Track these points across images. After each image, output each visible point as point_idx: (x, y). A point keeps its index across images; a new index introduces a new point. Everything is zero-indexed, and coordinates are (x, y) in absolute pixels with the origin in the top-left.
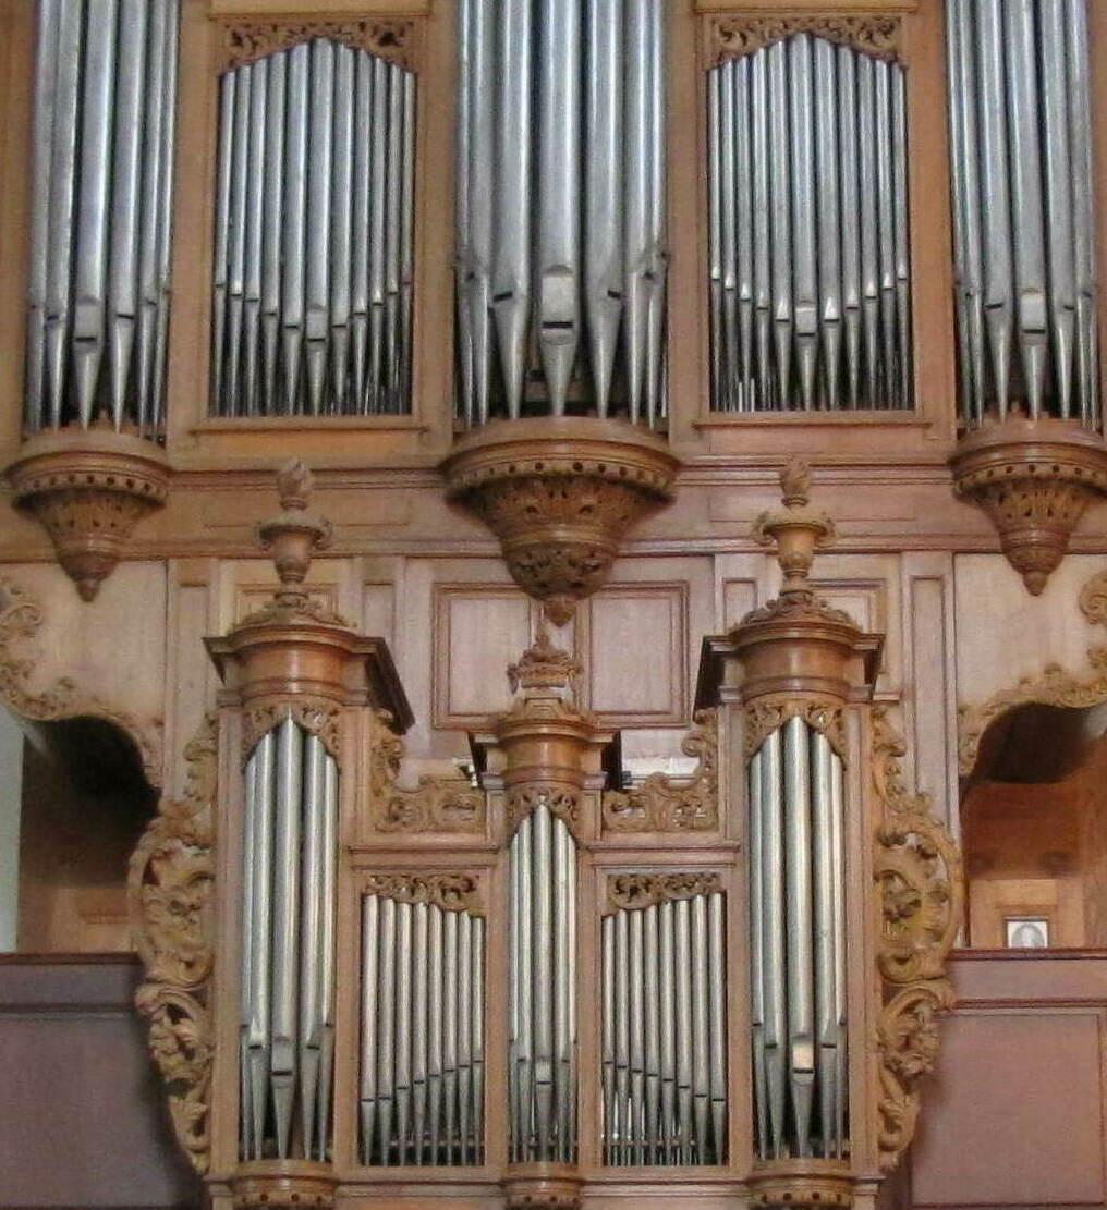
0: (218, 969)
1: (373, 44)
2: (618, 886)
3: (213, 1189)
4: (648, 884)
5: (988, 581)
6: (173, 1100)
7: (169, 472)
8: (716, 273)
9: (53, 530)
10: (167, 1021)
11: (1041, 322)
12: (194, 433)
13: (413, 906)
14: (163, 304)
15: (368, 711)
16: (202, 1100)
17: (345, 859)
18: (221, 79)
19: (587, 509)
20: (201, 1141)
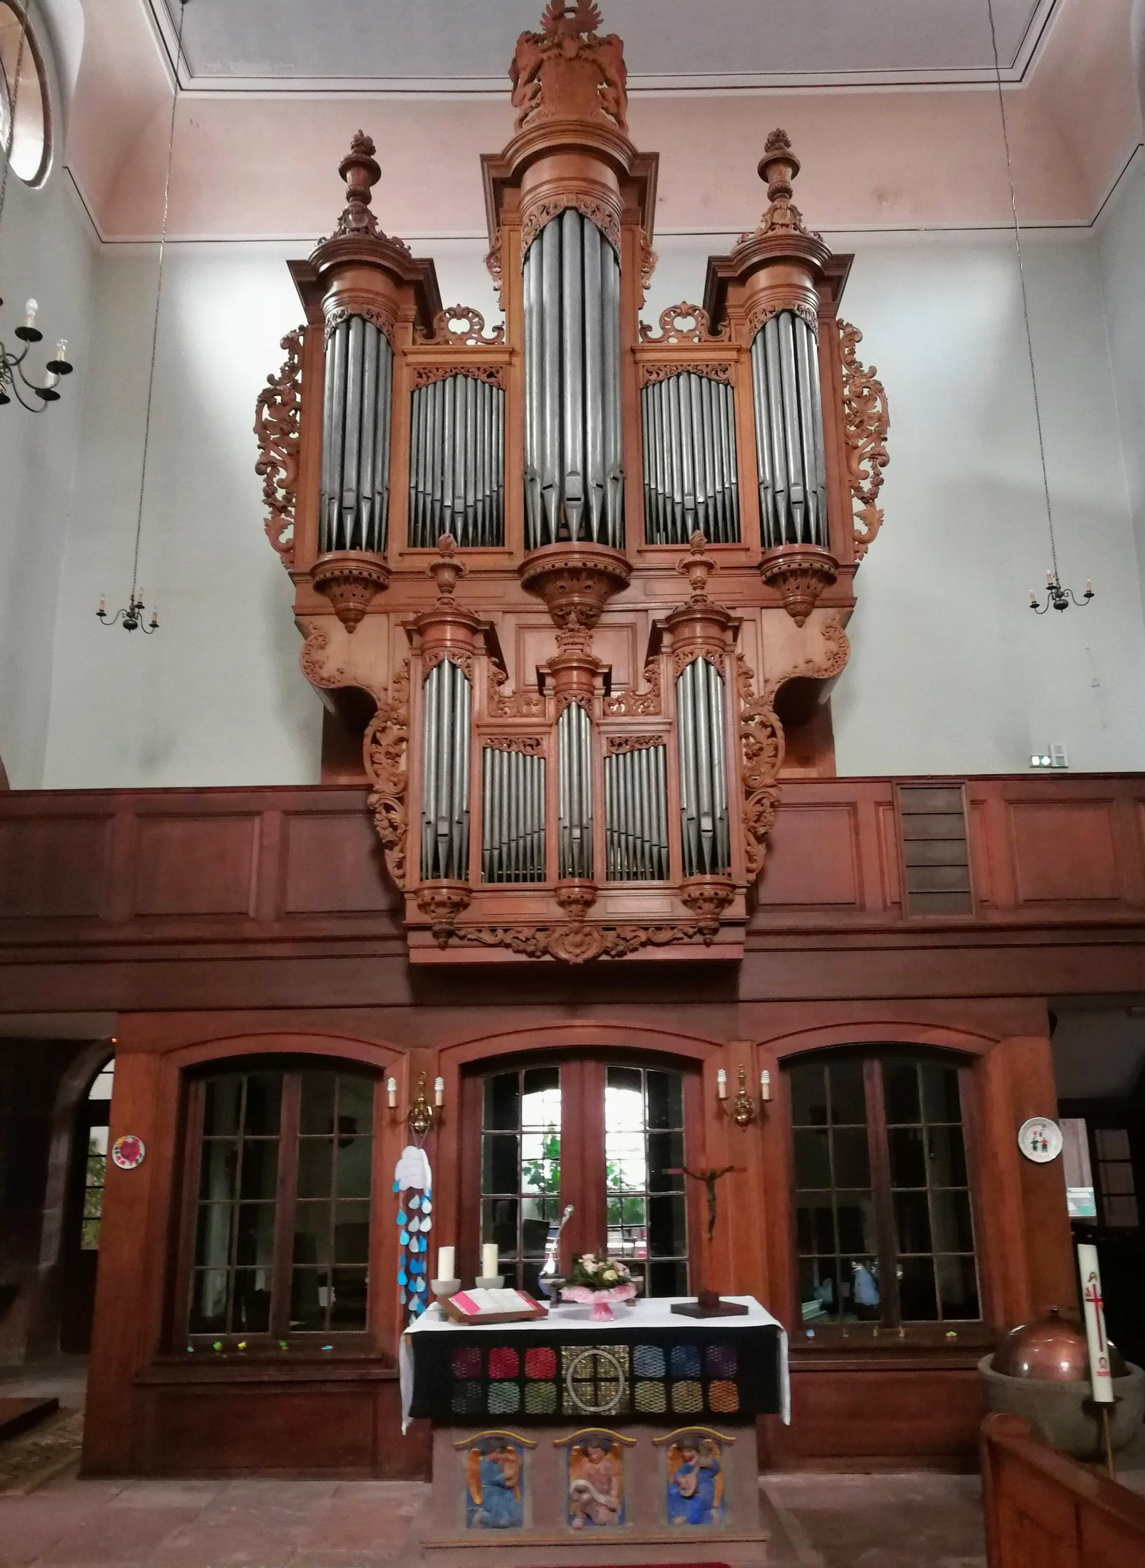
0: (410, 786)
1: (484, 377)
2: (612, 742)
3: (406, 896)
4: (626, 742)
5: (776, 623)
6: (387, 851)
7: (389, 572)
8: (647, 482)
9: (333, 600)
10: (384, 812)
11: (801, 498)
12: (401, 555)
13: (509, 753)
14: (385, 496)
15: (486, 658)
16: (402, 851)
17: (476, 731)
18: (412, 393)
19: (589, 587)
20: (400, 872)
